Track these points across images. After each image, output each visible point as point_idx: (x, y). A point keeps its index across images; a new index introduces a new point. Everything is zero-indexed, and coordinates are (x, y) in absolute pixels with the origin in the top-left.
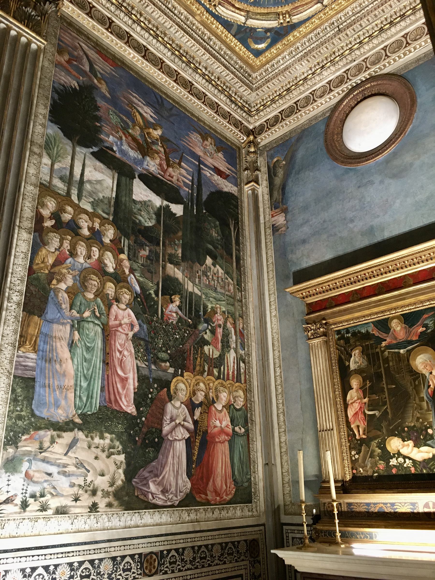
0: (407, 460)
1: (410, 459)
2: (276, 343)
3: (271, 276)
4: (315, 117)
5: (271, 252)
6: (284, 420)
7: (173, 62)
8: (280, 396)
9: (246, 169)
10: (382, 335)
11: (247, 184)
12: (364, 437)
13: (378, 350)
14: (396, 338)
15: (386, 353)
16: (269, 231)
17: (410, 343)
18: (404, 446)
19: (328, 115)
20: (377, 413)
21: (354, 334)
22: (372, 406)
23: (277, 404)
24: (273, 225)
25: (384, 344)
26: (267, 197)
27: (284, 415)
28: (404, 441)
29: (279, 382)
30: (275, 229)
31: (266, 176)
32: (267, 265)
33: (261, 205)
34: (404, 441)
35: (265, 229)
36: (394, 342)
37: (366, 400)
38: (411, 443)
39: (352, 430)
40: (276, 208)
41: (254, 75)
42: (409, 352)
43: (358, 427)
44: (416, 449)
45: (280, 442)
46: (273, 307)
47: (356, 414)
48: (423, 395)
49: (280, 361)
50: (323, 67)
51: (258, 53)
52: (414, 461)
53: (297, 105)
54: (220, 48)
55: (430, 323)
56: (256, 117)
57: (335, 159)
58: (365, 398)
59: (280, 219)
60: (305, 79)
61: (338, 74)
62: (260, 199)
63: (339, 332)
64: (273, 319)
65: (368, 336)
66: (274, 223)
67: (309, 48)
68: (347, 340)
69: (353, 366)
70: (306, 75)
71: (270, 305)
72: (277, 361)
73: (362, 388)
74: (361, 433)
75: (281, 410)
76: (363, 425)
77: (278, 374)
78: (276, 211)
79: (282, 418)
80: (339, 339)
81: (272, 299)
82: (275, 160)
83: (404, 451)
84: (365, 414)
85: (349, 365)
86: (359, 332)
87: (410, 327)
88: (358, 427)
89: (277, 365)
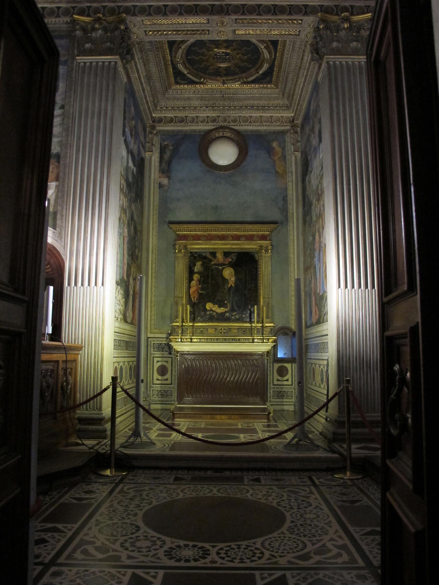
0: (214, 313)
1: (215, 312)
2: (154, 250)
3: (155, 212)
4: (195, 131)
5: (157, 198)
6: (155, 291)
7: (144, 78)
8: (154, 278)
9: (148, 142)
10: (213, 259)
11: (147, 152)
12: (196, 302)
13: (209, 265)
14: (218, 261)
15: (213, 267)
16: (157, 186)
17: (225, 265)
18: (214, 307)
19: (202, 133)
20: (204, 292)
21: (199, 255)
22: (202, 289)
23: (152, 282)
24: (160, 183)
25: (213, 263)
26: (157, 164)
27: (155, 288)
28: (214, 305)
29: (154, 270)
30: (161, 186)
31: (158, 151)
32: (153, 206)
33: (153, 167)
34: (214, 305)
35: (154, 183)
36: (218, 263)
37: (200, 286)
38: (217, 306)
39: (191, 298)
40: (163, 173)
41: (169, 91)
42: (223, 269)
43: (194, 297)
44: (219, 308)
45: (151, 301)
46: (155, 230)
47: (194, 292)
48: (226, 287)
49: (155, 260)
50: (207, 107)
51: (177, 83)
52: (217, 313)
53: (186, 119)
54: (164, 76)
55: (234, 258)
56: (159, 112)
57: (203, 161)
58: (200, 285)
59: (165, 181)
60: (195, 107)
61: (213, 115)
62: (153, 163)
63: (191, 253)
64: (154, 237)
65: (205, 258)
66: (160, 182)
67: (205, 96)
68: (195, 258)
69: (196, 270)
70: (197, 106)
71: (153, 229)
72: (154, 260)
73: (199, 281)
74: (195, 299)
75: (154, 285)
76: (196, 296)
77: (154, 267)
78: (163, 175)
79: (153, 289)
80: (191, 256)
81: (155, 226)
82: (166, 143)
83: (214, 309)
84: (198, 292)
85: (194, 270)
86: (202, 255)
87: (226, 258)
88: (194, 297)
89: (154, 262)
